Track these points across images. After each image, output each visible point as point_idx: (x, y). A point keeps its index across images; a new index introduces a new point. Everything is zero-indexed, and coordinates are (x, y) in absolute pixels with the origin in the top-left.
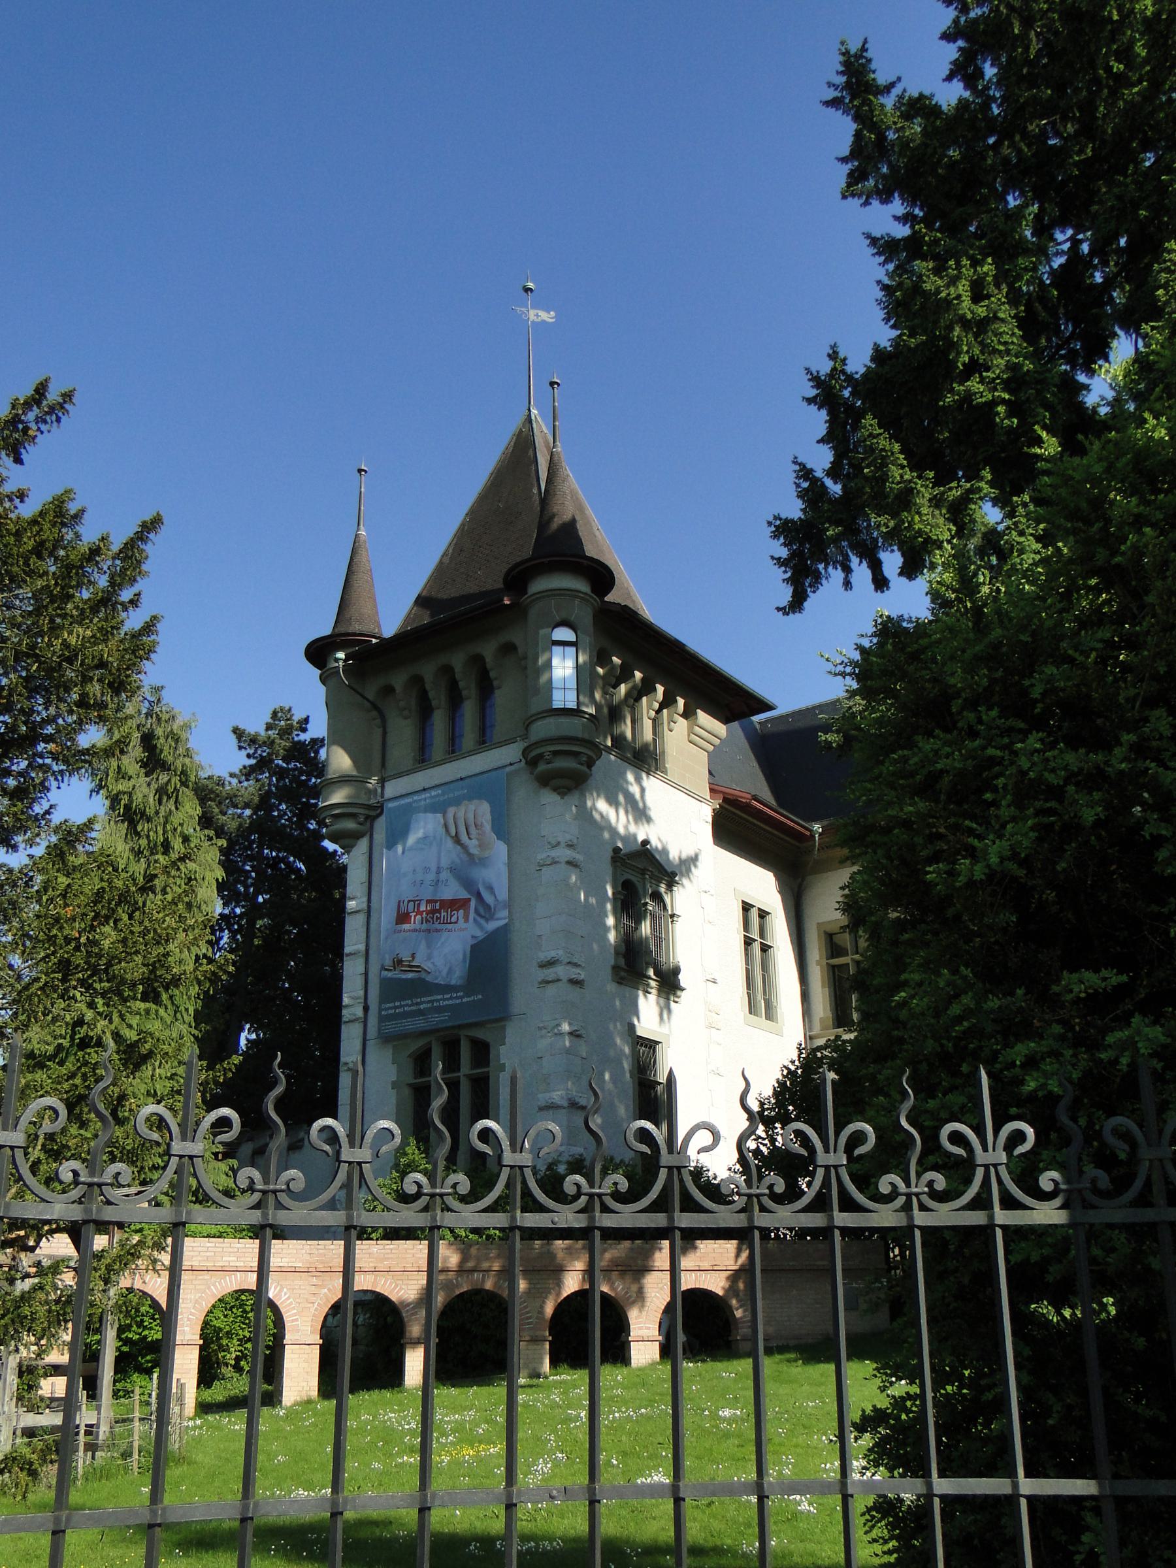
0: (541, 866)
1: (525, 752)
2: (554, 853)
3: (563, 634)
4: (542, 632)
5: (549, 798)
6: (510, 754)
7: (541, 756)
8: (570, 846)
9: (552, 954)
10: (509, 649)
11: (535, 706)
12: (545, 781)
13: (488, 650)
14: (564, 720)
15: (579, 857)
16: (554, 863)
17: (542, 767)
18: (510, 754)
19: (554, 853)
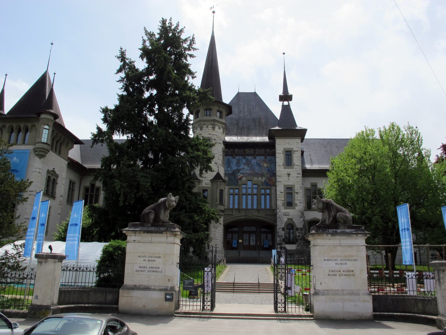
0: (33, 172)
1: (34, 149)
2: (36, 170)
3: (46, 127)
4: (42, 126)
5: (37, 158)
6: (31, 147)
7: (37, 151)
8: (40, 169)
9: (32, 190)
10: (34, 126)
11: (38, 140)
12: (37, 155)
13: (29, 125)
14: (43, 145)
15: (41, 171)
16: (36, 172)
17: (37, 153)
18: (31, 147)
19: (36, 170)
